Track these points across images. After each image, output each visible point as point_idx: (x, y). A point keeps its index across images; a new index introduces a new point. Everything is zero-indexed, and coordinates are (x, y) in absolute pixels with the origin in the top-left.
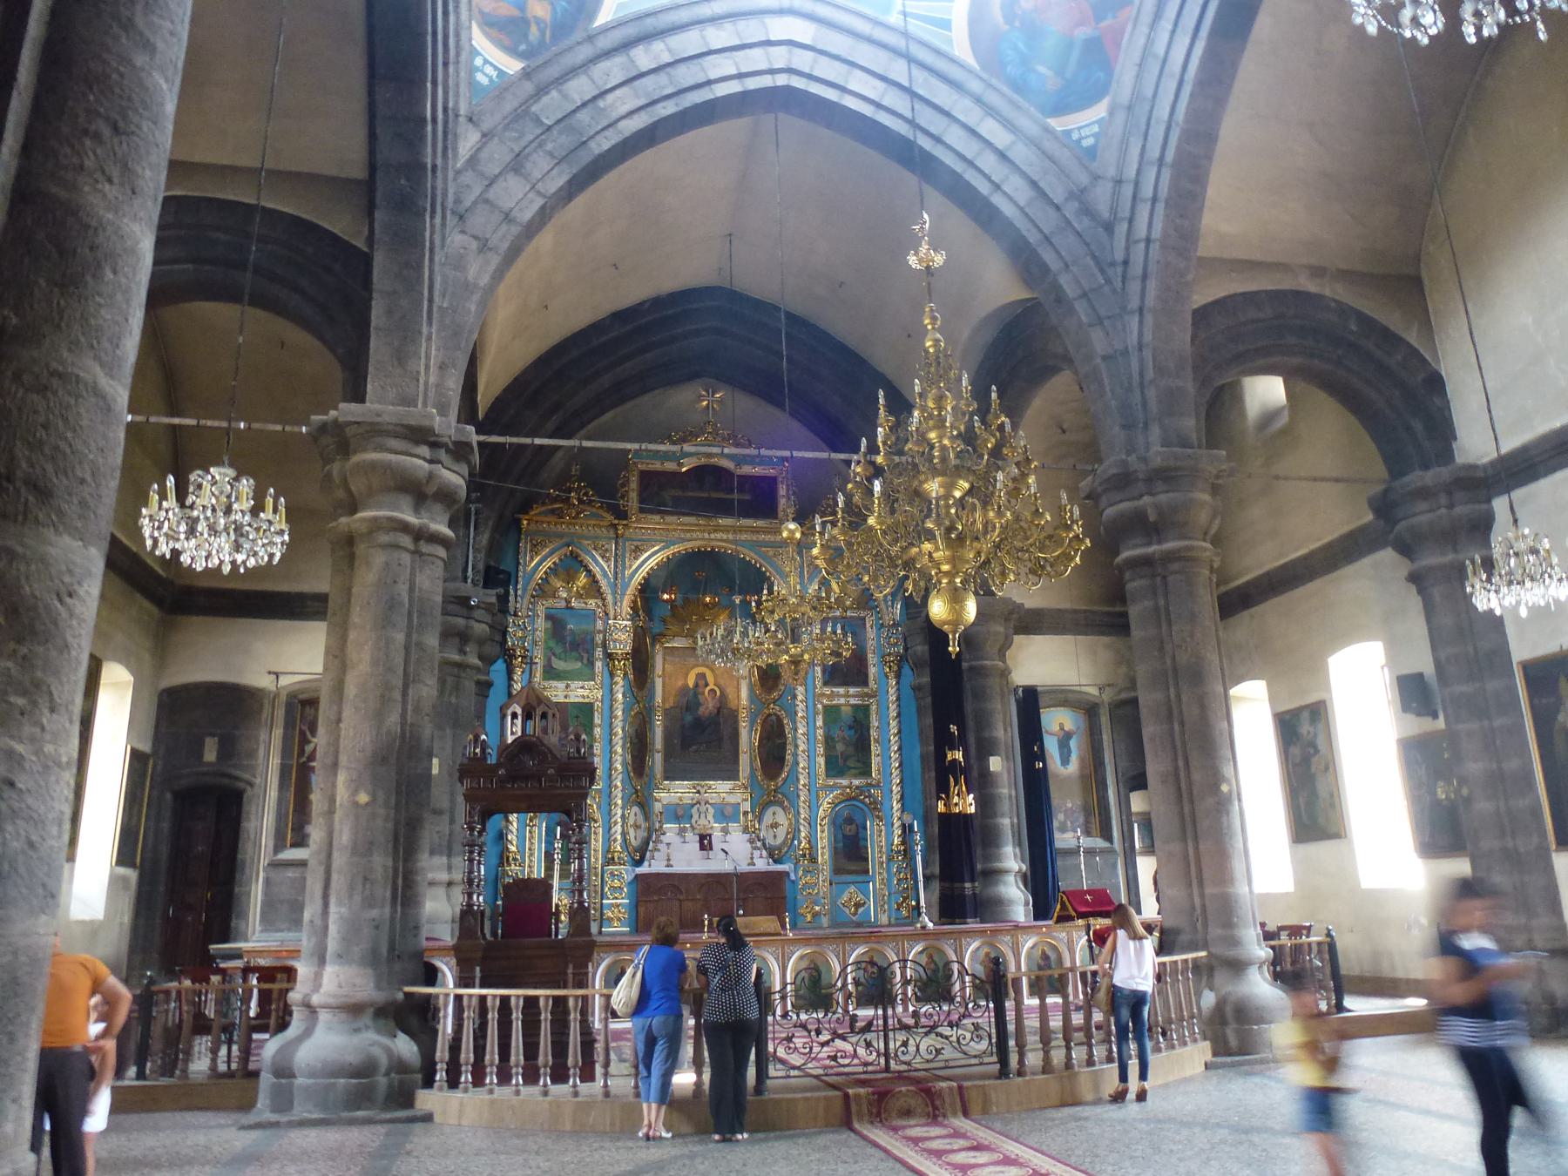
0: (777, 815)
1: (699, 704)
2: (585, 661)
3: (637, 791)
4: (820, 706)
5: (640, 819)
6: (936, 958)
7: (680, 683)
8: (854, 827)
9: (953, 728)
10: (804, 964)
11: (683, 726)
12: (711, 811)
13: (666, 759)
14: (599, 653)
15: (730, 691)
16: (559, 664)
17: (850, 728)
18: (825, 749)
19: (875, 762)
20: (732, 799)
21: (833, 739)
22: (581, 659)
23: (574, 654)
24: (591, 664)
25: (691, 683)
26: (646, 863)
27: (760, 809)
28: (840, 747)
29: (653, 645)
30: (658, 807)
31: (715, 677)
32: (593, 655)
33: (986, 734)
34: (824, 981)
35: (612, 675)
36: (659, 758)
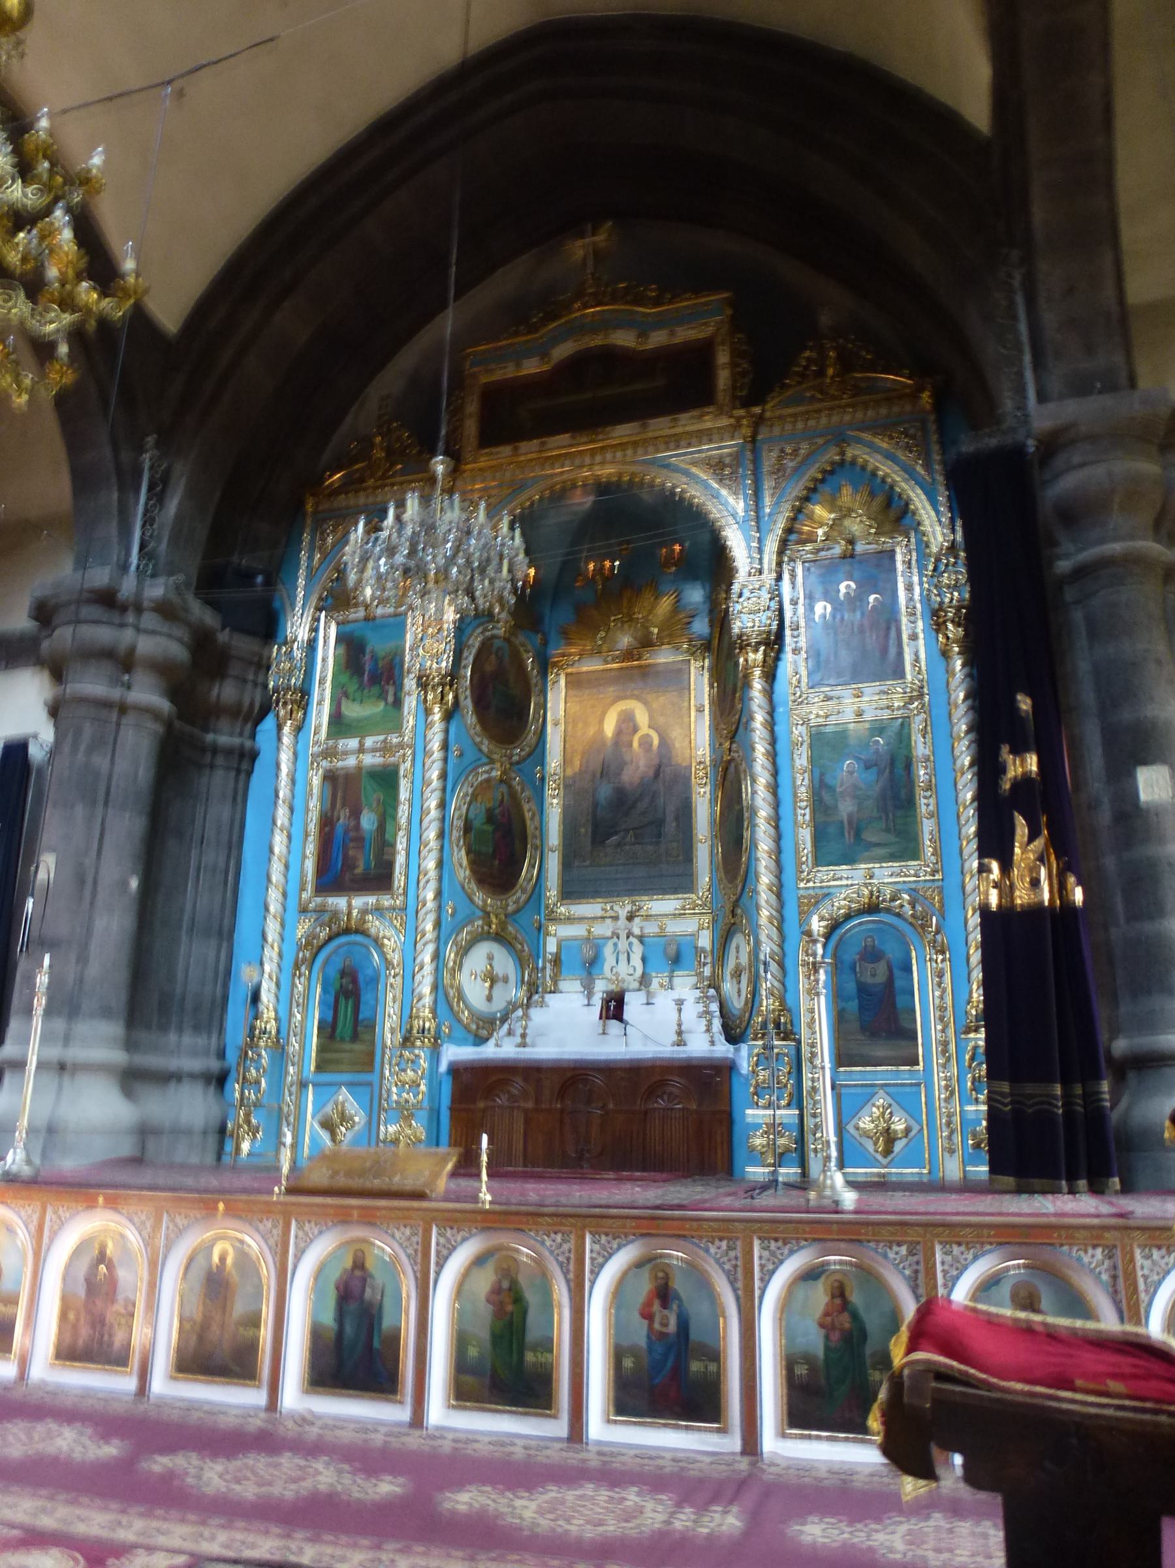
0: (739, 951)
1: (622, 765)
2: (390, 699)
3: (487, 914)
4: (802, 729)
5: (505, 964)
6: (856, 1298)
7: (591, 731)
8: (881, 968)
9: (1025, 704)
10: (484, 1281)
11: (595, 805)
12: (637, 950)
13: (566, 864)
14: (410, 683)
15: (676, 734)
16: (352, 710)
17: (868, 766)
18: (814, 812)
19: (928, 827)
20: (675, 928)
21: (831, 789)
22: (382, 696)
23: (375, 690)
24: (398, 703)
25: (609, 727)
26: (492, 1042)
27: (724, 939)
28: (846, 808)
29: (544, 673)
30: (551, 946)
31: (651, 718)
32: (399, 687)
33: (1126, 715)
34: (533, 1333)
35: (428, 712)
36: (553, 863)
